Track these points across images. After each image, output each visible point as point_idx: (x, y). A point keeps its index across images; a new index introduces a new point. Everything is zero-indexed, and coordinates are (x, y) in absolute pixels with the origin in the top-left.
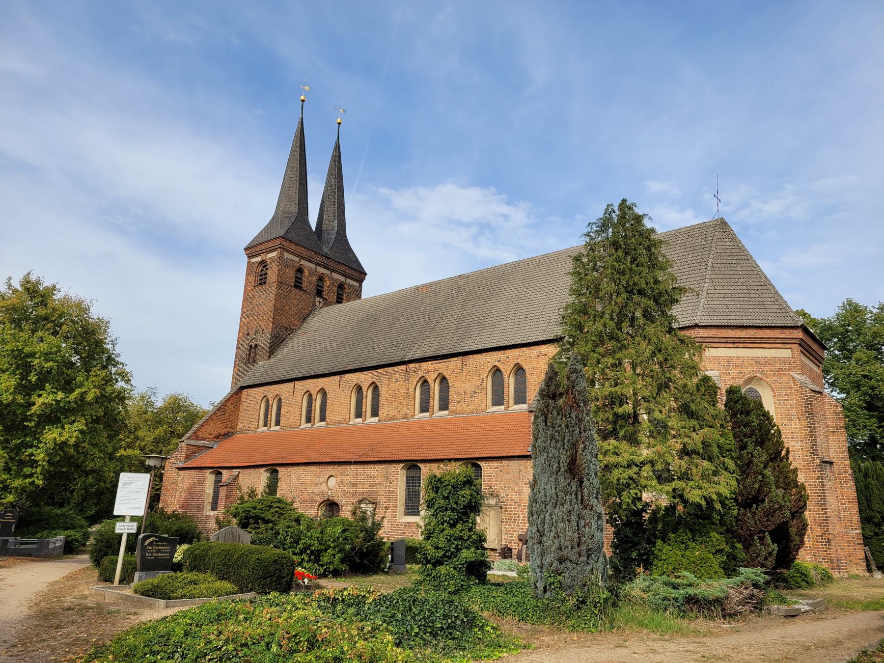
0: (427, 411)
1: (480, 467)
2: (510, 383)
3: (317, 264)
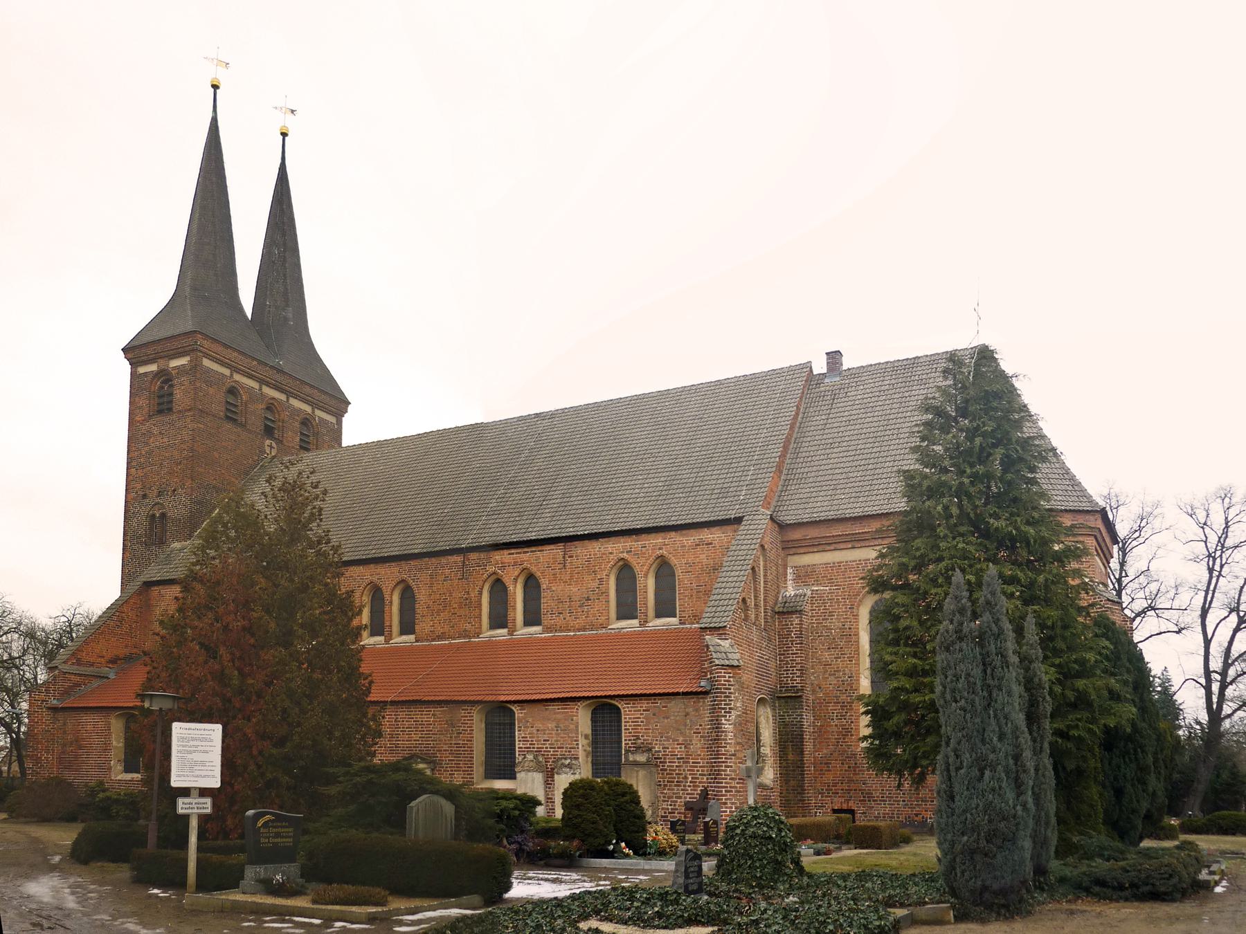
0: (503, 626)
1: (618, 709)
2: (648, 586)
3: (262, 382)
